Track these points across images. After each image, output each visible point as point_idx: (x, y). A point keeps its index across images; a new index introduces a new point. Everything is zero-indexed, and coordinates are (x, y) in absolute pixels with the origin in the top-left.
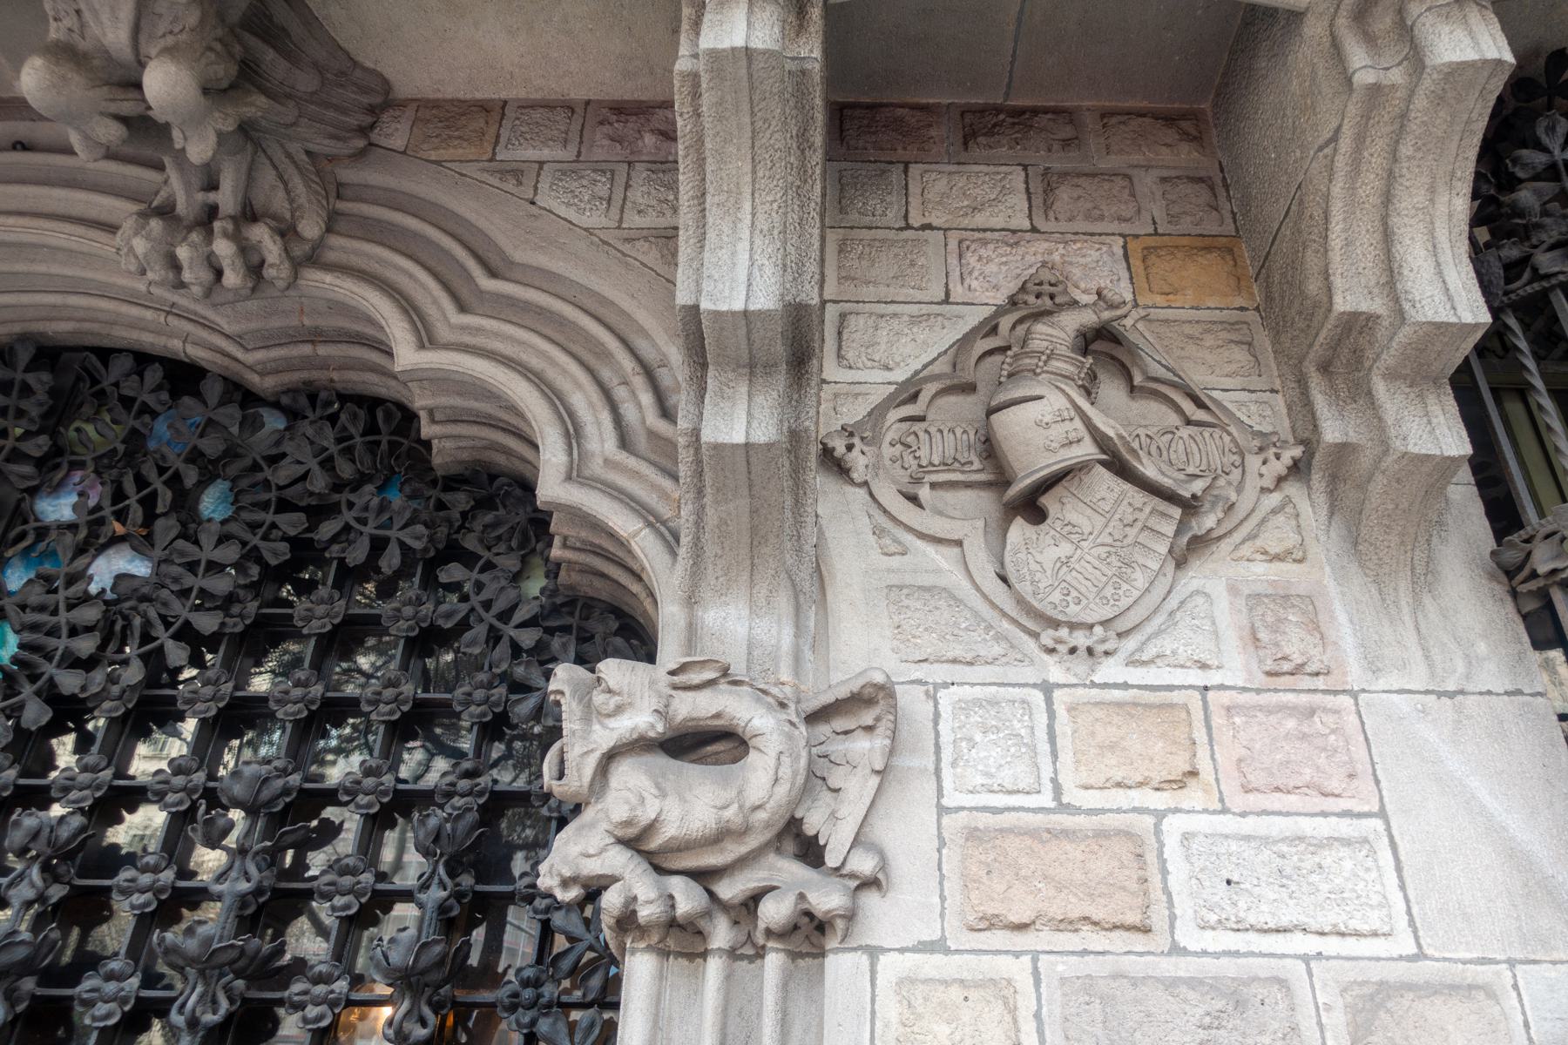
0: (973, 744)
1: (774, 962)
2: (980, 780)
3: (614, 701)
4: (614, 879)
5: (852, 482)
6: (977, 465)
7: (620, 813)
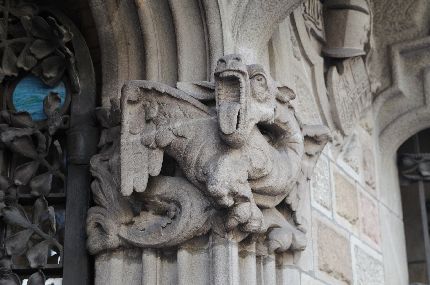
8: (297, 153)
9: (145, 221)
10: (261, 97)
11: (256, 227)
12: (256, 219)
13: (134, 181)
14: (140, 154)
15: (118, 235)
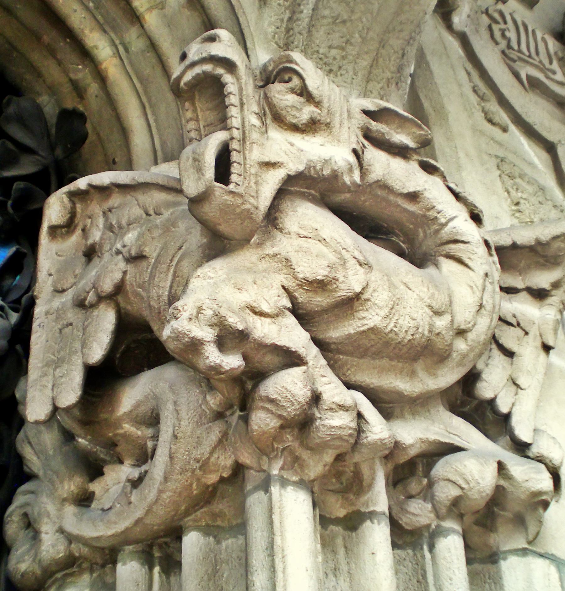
4: (292, 359)
5: (449, 26)
7: (311, 267)
8: (466, 265)
9: (114, 485)
10: (295, 117)
11: (340, 428)
12: (334, 406)
13: (53, 386)
14: (70, 327)
15: (61, 531)
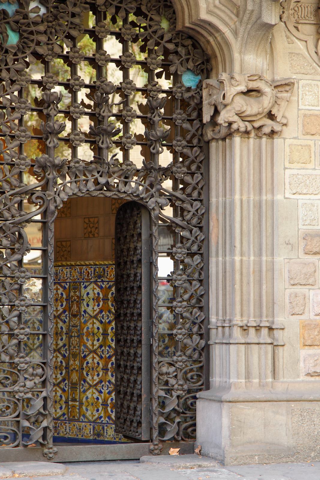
0: (306, 95)
1: (264, 139)
2: (307, 103)
3: (237, 83)
4: (235, 122)
6: (312, 19)
7: (238, 109)
